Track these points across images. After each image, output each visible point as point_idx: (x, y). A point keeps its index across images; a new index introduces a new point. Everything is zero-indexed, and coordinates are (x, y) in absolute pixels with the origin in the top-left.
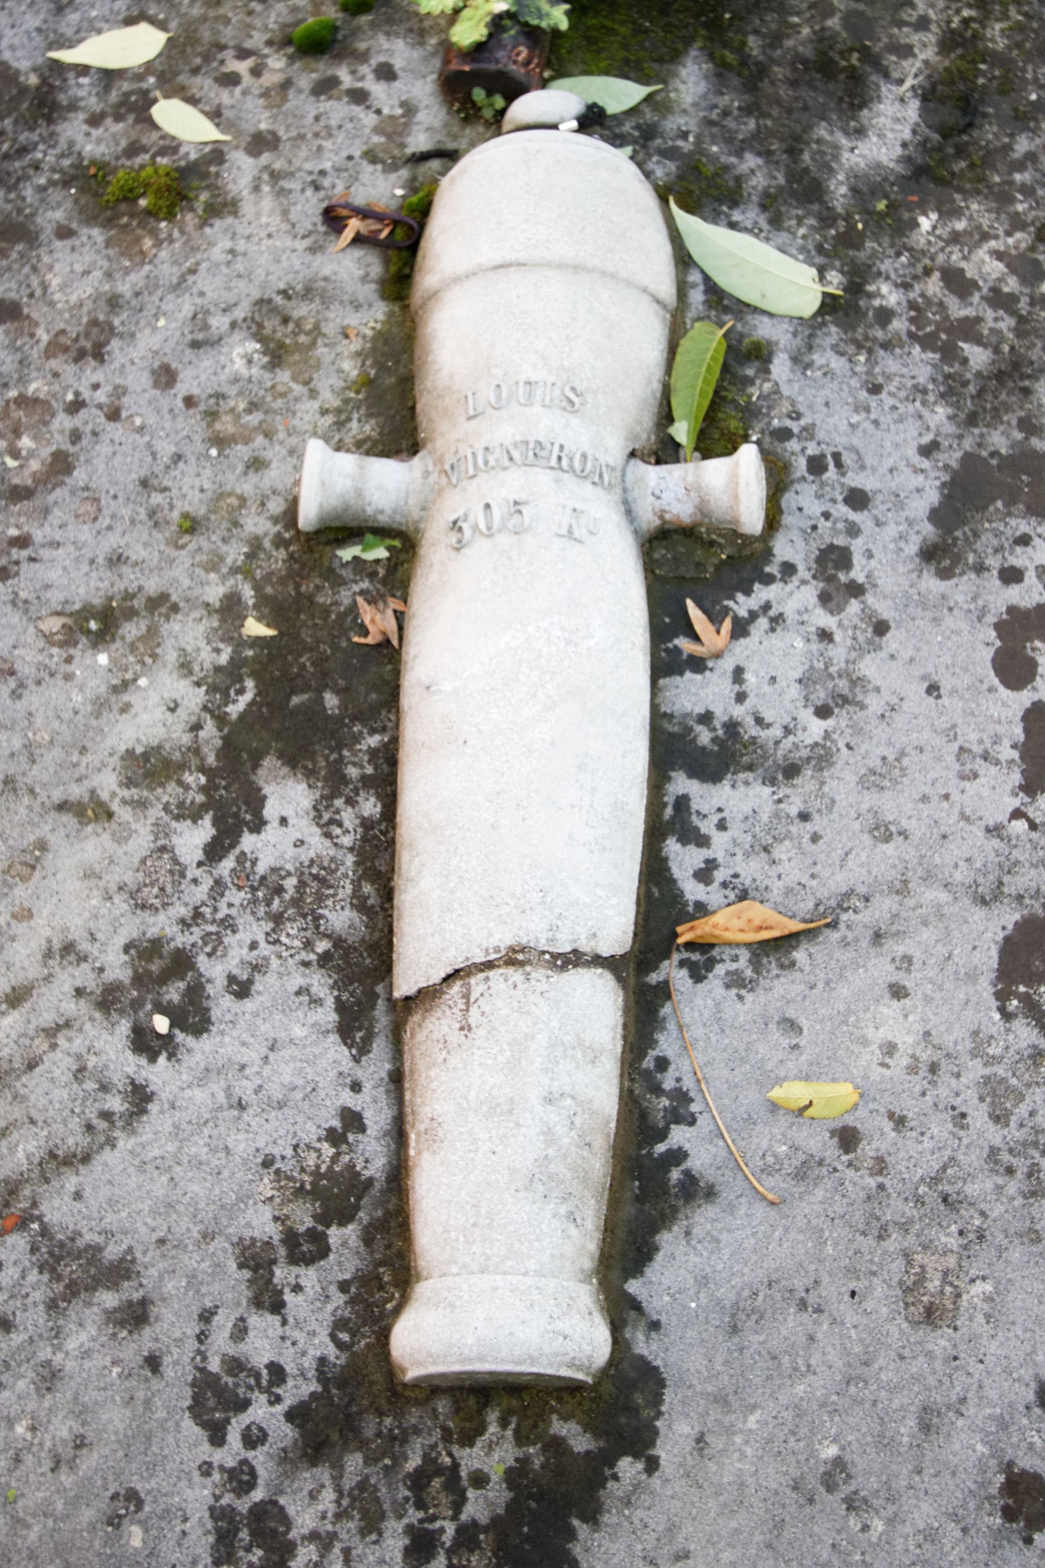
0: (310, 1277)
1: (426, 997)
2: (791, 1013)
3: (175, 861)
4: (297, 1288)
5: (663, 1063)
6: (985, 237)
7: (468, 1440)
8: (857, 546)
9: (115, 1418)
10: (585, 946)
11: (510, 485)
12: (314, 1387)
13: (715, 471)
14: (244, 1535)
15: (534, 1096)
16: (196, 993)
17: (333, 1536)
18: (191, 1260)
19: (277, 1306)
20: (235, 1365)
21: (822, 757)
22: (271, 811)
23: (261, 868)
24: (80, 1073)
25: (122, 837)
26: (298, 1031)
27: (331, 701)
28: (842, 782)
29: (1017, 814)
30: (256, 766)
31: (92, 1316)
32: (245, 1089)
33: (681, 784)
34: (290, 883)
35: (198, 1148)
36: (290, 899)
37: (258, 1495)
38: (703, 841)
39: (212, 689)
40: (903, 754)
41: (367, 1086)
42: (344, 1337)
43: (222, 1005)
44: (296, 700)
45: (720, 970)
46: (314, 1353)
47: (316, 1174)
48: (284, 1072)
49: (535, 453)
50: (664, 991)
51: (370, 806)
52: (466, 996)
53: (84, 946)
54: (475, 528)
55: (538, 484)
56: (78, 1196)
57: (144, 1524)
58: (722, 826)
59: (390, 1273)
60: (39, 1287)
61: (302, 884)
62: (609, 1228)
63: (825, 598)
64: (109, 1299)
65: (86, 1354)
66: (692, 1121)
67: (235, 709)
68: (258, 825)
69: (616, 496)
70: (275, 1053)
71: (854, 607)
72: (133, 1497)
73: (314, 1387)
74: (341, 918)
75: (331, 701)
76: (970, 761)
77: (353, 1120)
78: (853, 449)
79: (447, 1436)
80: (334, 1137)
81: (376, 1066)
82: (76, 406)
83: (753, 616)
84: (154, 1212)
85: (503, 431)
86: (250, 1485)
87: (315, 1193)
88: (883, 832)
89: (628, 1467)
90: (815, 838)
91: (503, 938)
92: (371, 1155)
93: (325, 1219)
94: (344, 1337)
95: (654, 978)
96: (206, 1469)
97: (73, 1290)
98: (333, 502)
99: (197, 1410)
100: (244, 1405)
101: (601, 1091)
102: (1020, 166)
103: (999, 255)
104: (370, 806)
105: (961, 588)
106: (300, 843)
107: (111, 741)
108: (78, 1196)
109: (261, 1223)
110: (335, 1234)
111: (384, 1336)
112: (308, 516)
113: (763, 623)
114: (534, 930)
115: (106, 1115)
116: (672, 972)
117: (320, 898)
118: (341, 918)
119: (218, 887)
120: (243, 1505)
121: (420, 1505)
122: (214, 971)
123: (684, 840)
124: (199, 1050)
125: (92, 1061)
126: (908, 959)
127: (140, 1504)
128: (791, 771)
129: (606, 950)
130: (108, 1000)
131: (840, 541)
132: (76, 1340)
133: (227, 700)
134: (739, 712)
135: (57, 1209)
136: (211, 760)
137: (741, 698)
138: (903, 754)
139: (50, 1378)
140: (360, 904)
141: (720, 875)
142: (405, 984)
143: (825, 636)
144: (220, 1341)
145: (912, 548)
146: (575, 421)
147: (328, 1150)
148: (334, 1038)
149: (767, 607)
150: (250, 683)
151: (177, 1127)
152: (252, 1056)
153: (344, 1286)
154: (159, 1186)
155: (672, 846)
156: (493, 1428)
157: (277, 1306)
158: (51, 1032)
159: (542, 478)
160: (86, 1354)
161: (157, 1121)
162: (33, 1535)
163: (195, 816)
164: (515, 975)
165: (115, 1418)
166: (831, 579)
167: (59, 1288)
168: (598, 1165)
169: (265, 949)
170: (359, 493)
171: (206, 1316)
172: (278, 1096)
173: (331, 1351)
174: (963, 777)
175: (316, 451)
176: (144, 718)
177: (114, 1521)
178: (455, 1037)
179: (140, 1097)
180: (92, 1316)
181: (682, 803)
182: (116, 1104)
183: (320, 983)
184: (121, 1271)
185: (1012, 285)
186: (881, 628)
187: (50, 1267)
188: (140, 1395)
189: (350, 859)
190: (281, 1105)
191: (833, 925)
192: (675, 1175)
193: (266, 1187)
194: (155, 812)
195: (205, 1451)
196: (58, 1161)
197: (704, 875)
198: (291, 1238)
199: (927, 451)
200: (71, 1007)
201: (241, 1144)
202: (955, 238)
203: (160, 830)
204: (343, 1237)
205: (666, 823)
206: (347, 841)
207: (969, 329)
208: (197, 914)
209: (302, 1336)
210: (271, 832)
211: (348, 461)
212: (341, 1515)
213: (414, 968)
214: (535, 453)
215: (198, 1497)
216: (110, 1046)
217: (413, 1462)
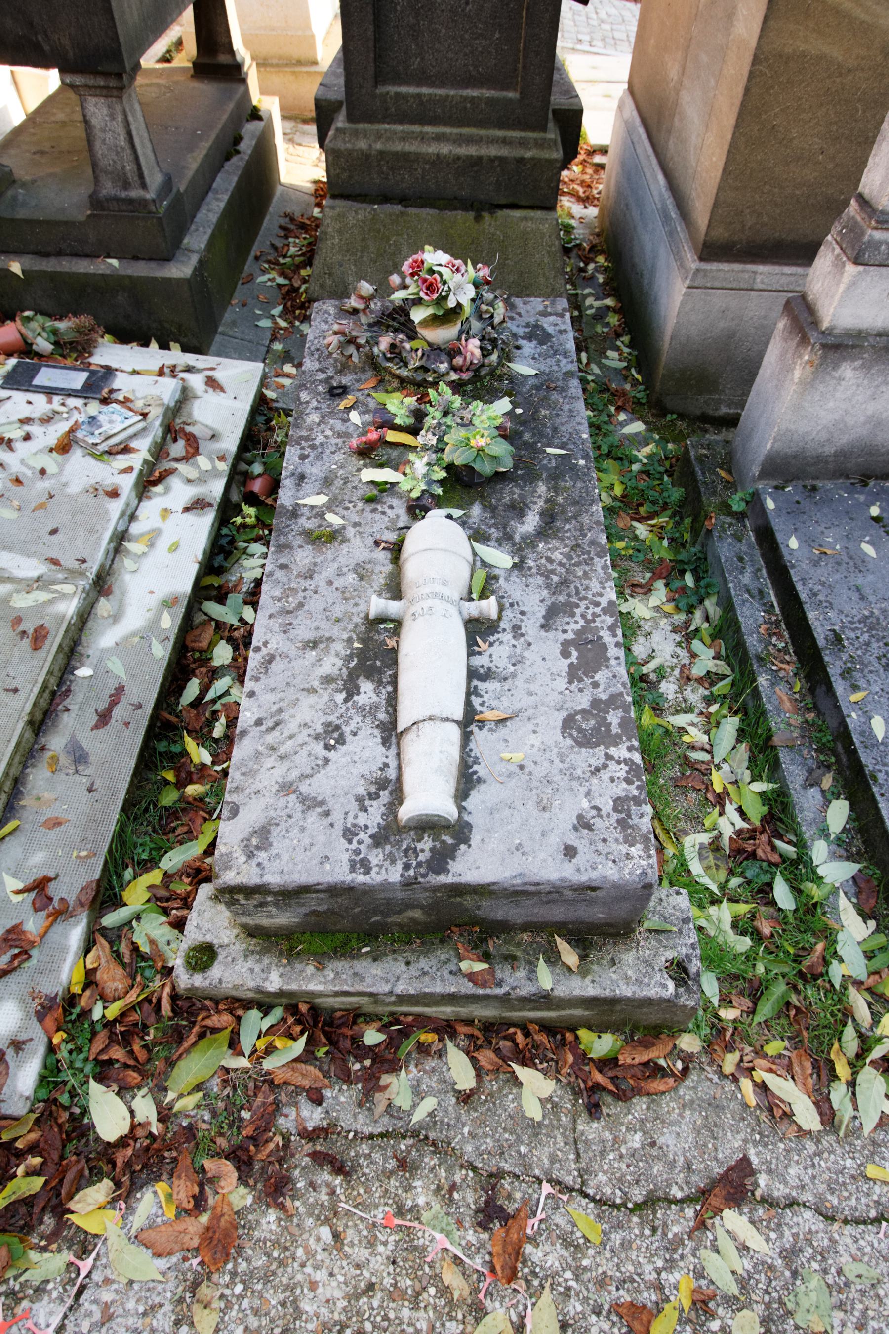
0: (375, 803)
7: (419, 841)
9: (322, 838)
13: (484, 603)
16: (342, 735)
18: (342, 800)
19: (366, 811)
20: (355, 825)
21: (514, 675)
25: (320, 697)
27: (378, 663)
28: (519, 681)
32: (356, 758)
33: (475, 682)
35: (343, 772)
43: (349, 738)
48: (367, 754)
49: (435, 595)
50: (471, 733)
51: (390, 689)
60: (299, 807)
62: (457, 789)
67: (351, 665)
68: (358, 694)
70: (365, 750)
72: (327, 857)
74: (382, 716)
75: (378, 663)
76: (553, 676)
77: (386, 765)
80: (381, 769)
81: (393, 750)
82: (305, 590)
85: (426, 590)
88: (531, 694)
91: (428, 714)
92: (392, 774)
97: (309, 808)
99: (344, 835)
101: (455, 753)
104: (390, 689)
105: (551, 635)
109: (362, 791)
110: (381, 793)
112: (372, 616)
114: (436, 712)
116: (473, 728)
118: (382, 716)
119: (348, 709)
122: (347, 730)
124: (342, 749)
128: (505, 679)
130: (317, 737)
135: (304, 788)
139: (303, 829)
140: (387, 713)
142: (400, 728)
152: (358, 750)
154: (333, 782)
155: (473, 698)
157: (366, 811)
158: (301, 745)
161: (331, 767)
165: (322, 838)
168: (454, 771)
175: (374, 598)
177: (322, 863)
179: (327, 761)
181: (476, 687)
182: (320, 762)
183: (377, 732)
184: (322, 803)
186: (529, 644)
187: (302, 802)
193: (362, 781)
195: (347, 845)
196: (304, 777)
197: (482, 704)
198: (369, 794)
200: (307, 739)
201: (355, 771)
205: (471, 692)
207: (553, 572)
209: (374, 816)
210: (362, 695)
211: (383, 601)
214: (435, 595)
215: (345, 857)
216: (318, 748)
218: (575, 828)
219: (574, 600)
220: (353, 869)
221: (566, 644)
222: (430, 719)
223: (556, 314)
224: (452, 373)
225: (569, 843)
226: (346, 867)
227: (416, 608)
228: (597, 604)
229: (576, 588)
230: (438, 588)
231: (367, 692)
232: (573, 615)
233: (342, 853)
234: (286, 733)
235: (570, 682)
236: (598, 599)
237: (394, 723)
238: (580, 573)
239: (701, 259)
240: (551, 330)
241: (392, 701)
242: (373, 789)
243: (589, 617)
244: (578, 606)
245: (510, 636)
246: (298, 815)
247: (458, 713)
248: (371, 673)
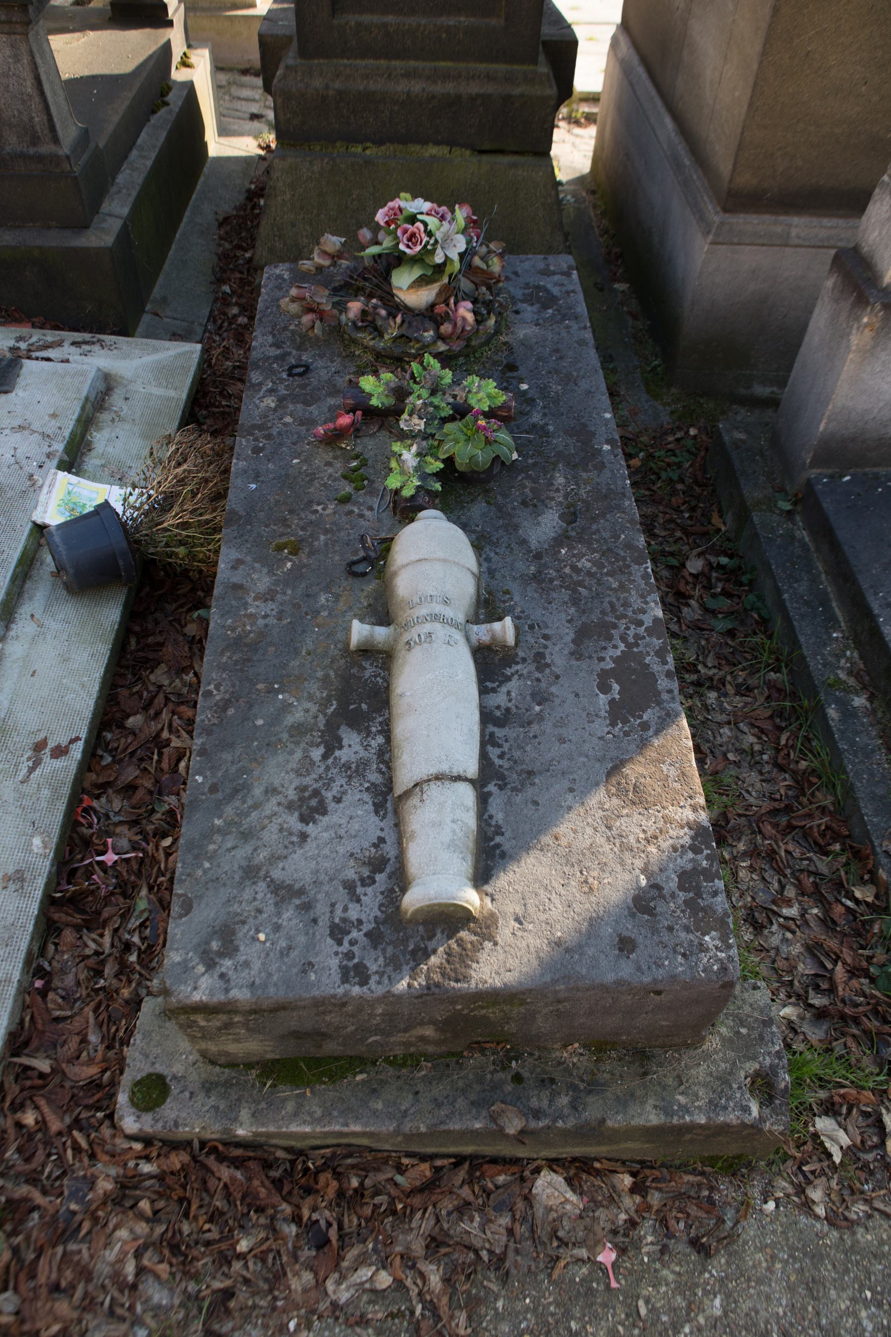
0: (369, 890)
1: (408, 794)
2: (536, 798)
3: (311, 760)
4: (365, 894)
5: (491, 817)
6: (584, 555)
7: (430, 938)
8: (547, 652)
9: (302, 939)
10: (462, 774)
11: (427, 627)
12: (373, 925)
13: (497, 626)
14: (352, 973)
16: (322, 802)
17: (384, 972)
18: (326, 888)
19: (358, 901)
20: (344, 920)
21: (540, 717)
22: (345, 742)
23: (342, 761)
24: (281, 830)
25: (291, 753)
26: (360, 813)
27: (364, 706)
28: (548, 726)
29: (608, 733)
30: (338, 728)
31: (291, 908)
32: (342, 832)
33: (491, 728)
34: (353, 766)
35: (326, 851)
37: (356, 961)
38: (500, 746)
39: (321, 705)
40: (568, 716)
41: (386, 829)
42: (383, 909)
43: (331, 806)
44: (352, 707)
45: (509, 786)
46: (372, 915)
47: (370, 857)
48: (356, 826)
50: (489, 794)
51: (380, 740)
52: (422, 791)
53: (280, 789)
54: (415, 642)
55: (437, 628)
56: (283, 869)
57: (315, 972)
58: (506, 741)
59: (401, 880)
60: (271, 899)
61: (358, 766)
62: (476, 868)
63: (538, 669)
64: (297, 902)
65: (290, 919)
66: (503, 834)
67: (330, 710)
68: (341, 747)
69: (463, 633)
70: (352, 819)
71: (547, 671)
72: (311, 964)
73: (373, 925)
74: (374, 777)
75: (364, 706)
76: (591, 717)
77: (382, 840)
78: (543, 622)
79: (422, 938)
80: (375, 845)
81: (390, 820)
82: (266, 616)
83: (513, 675)
84: (312, 873)
85: (423, 611)
86: (353, 957)
87: (370, 864)
88: (562, 740)
89: (488, 945)
90: (539, 743)
91: (433, 771)
92: (389, 850)
93: (374, 872)
94: (383, 909)
95: (486, 790)
96: (336, 954)
97: (283, 900)
99: (332, 935)
100: (349, 932)
101: (471, 821)
102: (595, 534)
103: (589, 561)
104: (380, 740)
105: (584, 664)
106: (356, 753)
107: (285, 723)
108: (283, 869)
109: (350, 874)
110: (378, 877)
111: (398, 908)
113: (516, 677)
114: (444, 768)
115: (292, 843)
116: (491, 787)
117: (365, 770)
118: (374, 777)
119: (328, 768)
120: (351, 964)
121: (414, 960)
122: (329, 795)
123: (493, 746)
124: (325, 820)
125: (285, 826)
126: (574, 780)
127: (313, 966)
128: (530, 723)
129: (469, 776)
130: (290, 807)
131: (541, 650)
132: (286, 915)
133: (326, 708)
134: (509, 705)
135: (277, 874)
136: (322, 728)
137: (510, 701)
138: (568, 716)
139: (277, 928)
140: (380, 771)
141: (507, 757)
142: (399, 790)
143: (538, 680)
144: (339, 912)
145: (566, 652)
147: (373, 850)
148: (373, 814)
149: (517, 671)
150: (334, 702)
151: (318, 845)
152: (343, 821)
153: (382, 893)
156: (439, 935)
157: (358, 901)
158: (270, 817)
159: (438, 626)
160: (290, 919)
161: (310, 847)
162: (275, 978)
163: (318, 745)
165: (302, 939)
166: (539, 662)
167: (278, 899)
168: (471, 845)
169: (346, 787)
170: (372, 636)
171: (333, 905)
172: (354, 833)
173: (379, 914)
174: (589, 722)
175: (356, 625)
176: (297, 715)
177: (304, 972)
178: (419, 804)
179: (304, 836)
180: (291, 908)
181: (492, 735)
182: (295, 839)
183: (366, 797)
184: (301, 892)
185: (594, 569)
186: (557, 677)
188: (311, 932)
189: (375, 757)
190: (355, 837)
191: (548, 770)
192: (498, 852)
193: (352, 863)
194: (303, 745)
195: (335, 948)
196: (274, 859)
197: (501, 757)
199: (569, 621)
200: (276, 809)
201: (341, 850)
202: (574, 556)
203: (305, 751)
204: (380, 877)
206: (373, 751)
207: (581, 584)
208: (320, 777)
209: (368, 908)
210: (345, 750)
211: (367, 627)
212: (385, 966)
215: (334, 962)
216: (293, 821)
217: (411, 947)
218: (633, 915)
219: (610, 619)
220: (345, 979)
222: (439, 778)
223: (563, 274)
224: (440, 343)
225: (626, 933)
226: (336, 977)
227: (412, 634)
228: (640, 623)
229: (610, 603)
230: (438, 608)
231: (353, 747)
232: (610, 638)
233: (329, 957)
234: (250, 802)
235: (613, 724)
236: (641, 616)
237: (389, 783)
238: (615, 585)
239: (725, 210)
240: (555, 291)
241: (386, 756)
242: (366, 872)
243: (631, 640)
244: (615, 626)
245: (533, 667)
246: (270, 909)
247: (472, 768)
248: (357, 721)
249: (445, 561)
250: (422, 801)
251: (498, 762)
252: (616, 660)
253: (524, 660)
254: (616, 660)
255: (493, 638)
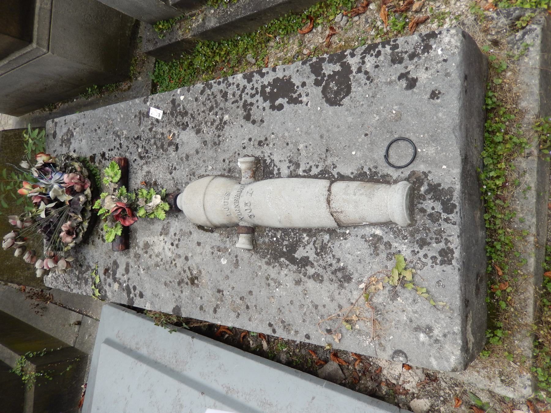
10: (327, 189)
11: (242, 205)
15: (354, 198)
16: (340, 269)
36: (322, 250)
38: (311, 167)
49: (237, 201)
50: (338, 173)
77: (363, 237)
85: (233, 207)
91: (325, 204)
95: (336, 176)
98: (247, 242)
101: (356, 184)
112: (250, 247)
113: (272, 157)
114: (323, 199)
116: (335, 172)
120: (439, 258)
129: (328, 185)
137: (285, 161)
146: (232, 193)
155: (312, 173)
159: (241, 199)
164: (331, 202)
197: (317, 166)
205: (308, 174)
213: (330, 223)
214: (237, 201)
219: (241, 104)
221: (273, 107)
222: (329, 202)
223: (56, 126)
224: (86, 193)
228: (245, 87)
230: (231, 199)
232: (252, 104)
235: (301, 102)
236: (241, 87)
237: (331, 232)
239: (31, 42)
240: (65, 130)
243: (254, 92)
244: (246, 101)
247: (324, 183)
249: (205, 194)
250: (342, 212)
251: (320, 168)
252: (265, 100)
253: (262, 152)
254: (265, 100)
255: (250, 169)
